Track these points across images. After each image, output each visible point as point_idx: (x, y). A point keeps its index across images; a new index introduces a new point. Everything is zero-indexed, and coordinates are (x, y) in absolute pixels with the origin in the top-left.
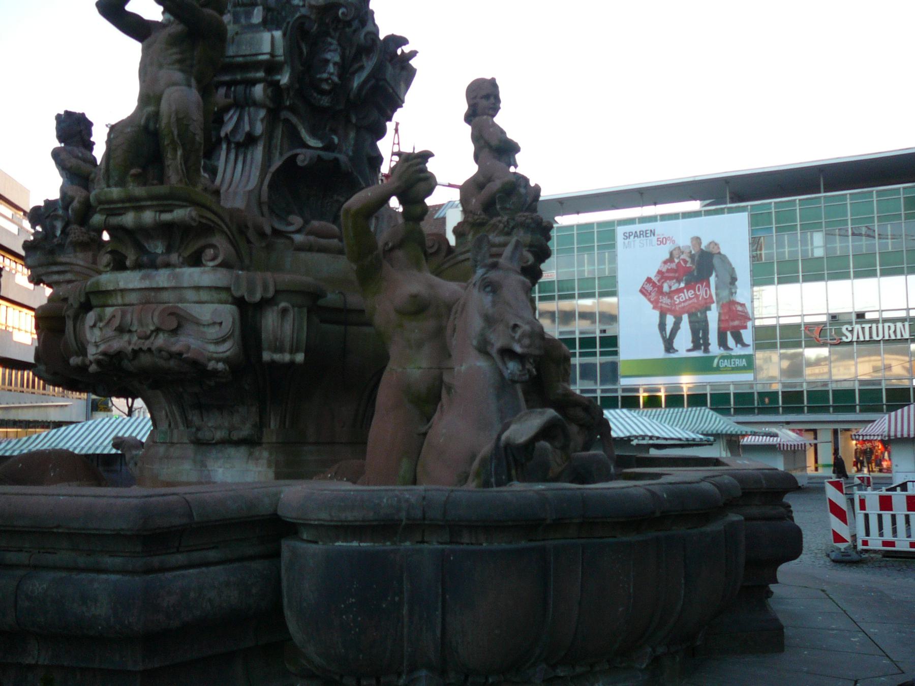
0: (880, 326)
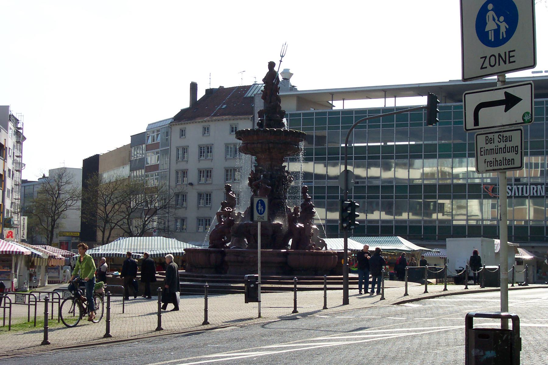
0: (528, 187)
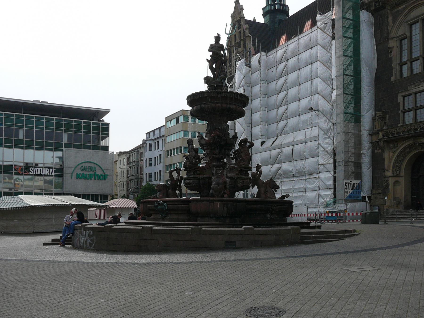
0: (44, 169)
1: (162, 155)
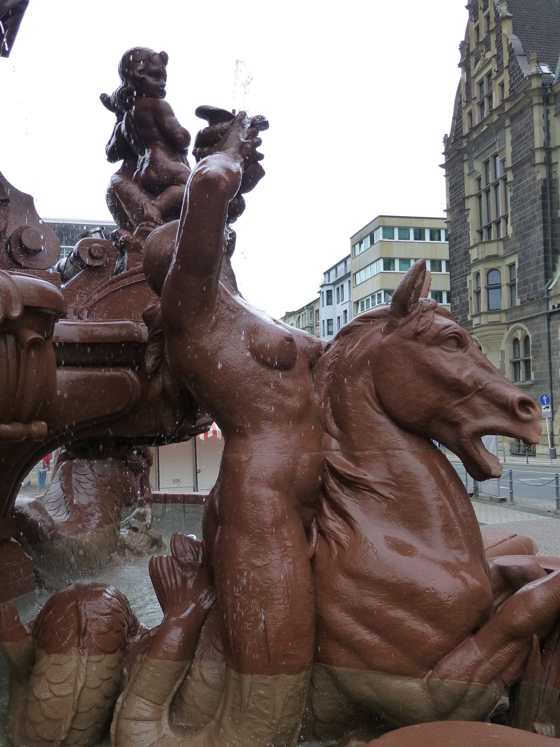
1: (348, 312)
